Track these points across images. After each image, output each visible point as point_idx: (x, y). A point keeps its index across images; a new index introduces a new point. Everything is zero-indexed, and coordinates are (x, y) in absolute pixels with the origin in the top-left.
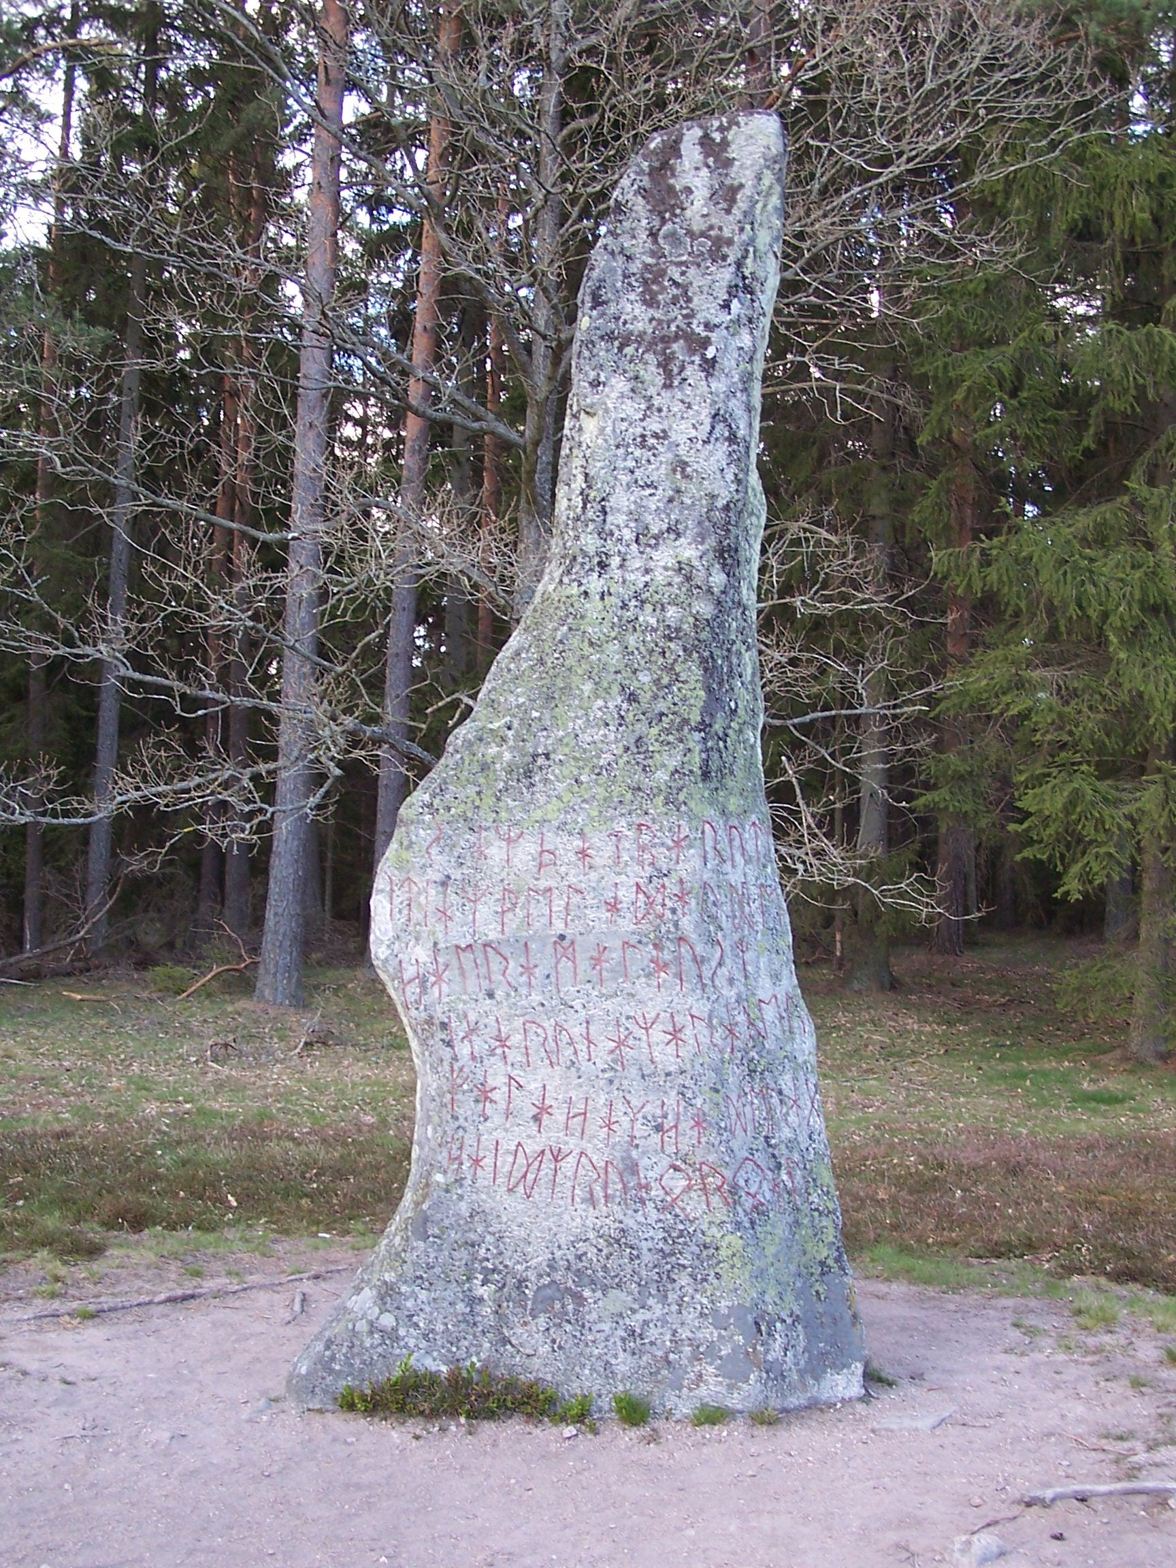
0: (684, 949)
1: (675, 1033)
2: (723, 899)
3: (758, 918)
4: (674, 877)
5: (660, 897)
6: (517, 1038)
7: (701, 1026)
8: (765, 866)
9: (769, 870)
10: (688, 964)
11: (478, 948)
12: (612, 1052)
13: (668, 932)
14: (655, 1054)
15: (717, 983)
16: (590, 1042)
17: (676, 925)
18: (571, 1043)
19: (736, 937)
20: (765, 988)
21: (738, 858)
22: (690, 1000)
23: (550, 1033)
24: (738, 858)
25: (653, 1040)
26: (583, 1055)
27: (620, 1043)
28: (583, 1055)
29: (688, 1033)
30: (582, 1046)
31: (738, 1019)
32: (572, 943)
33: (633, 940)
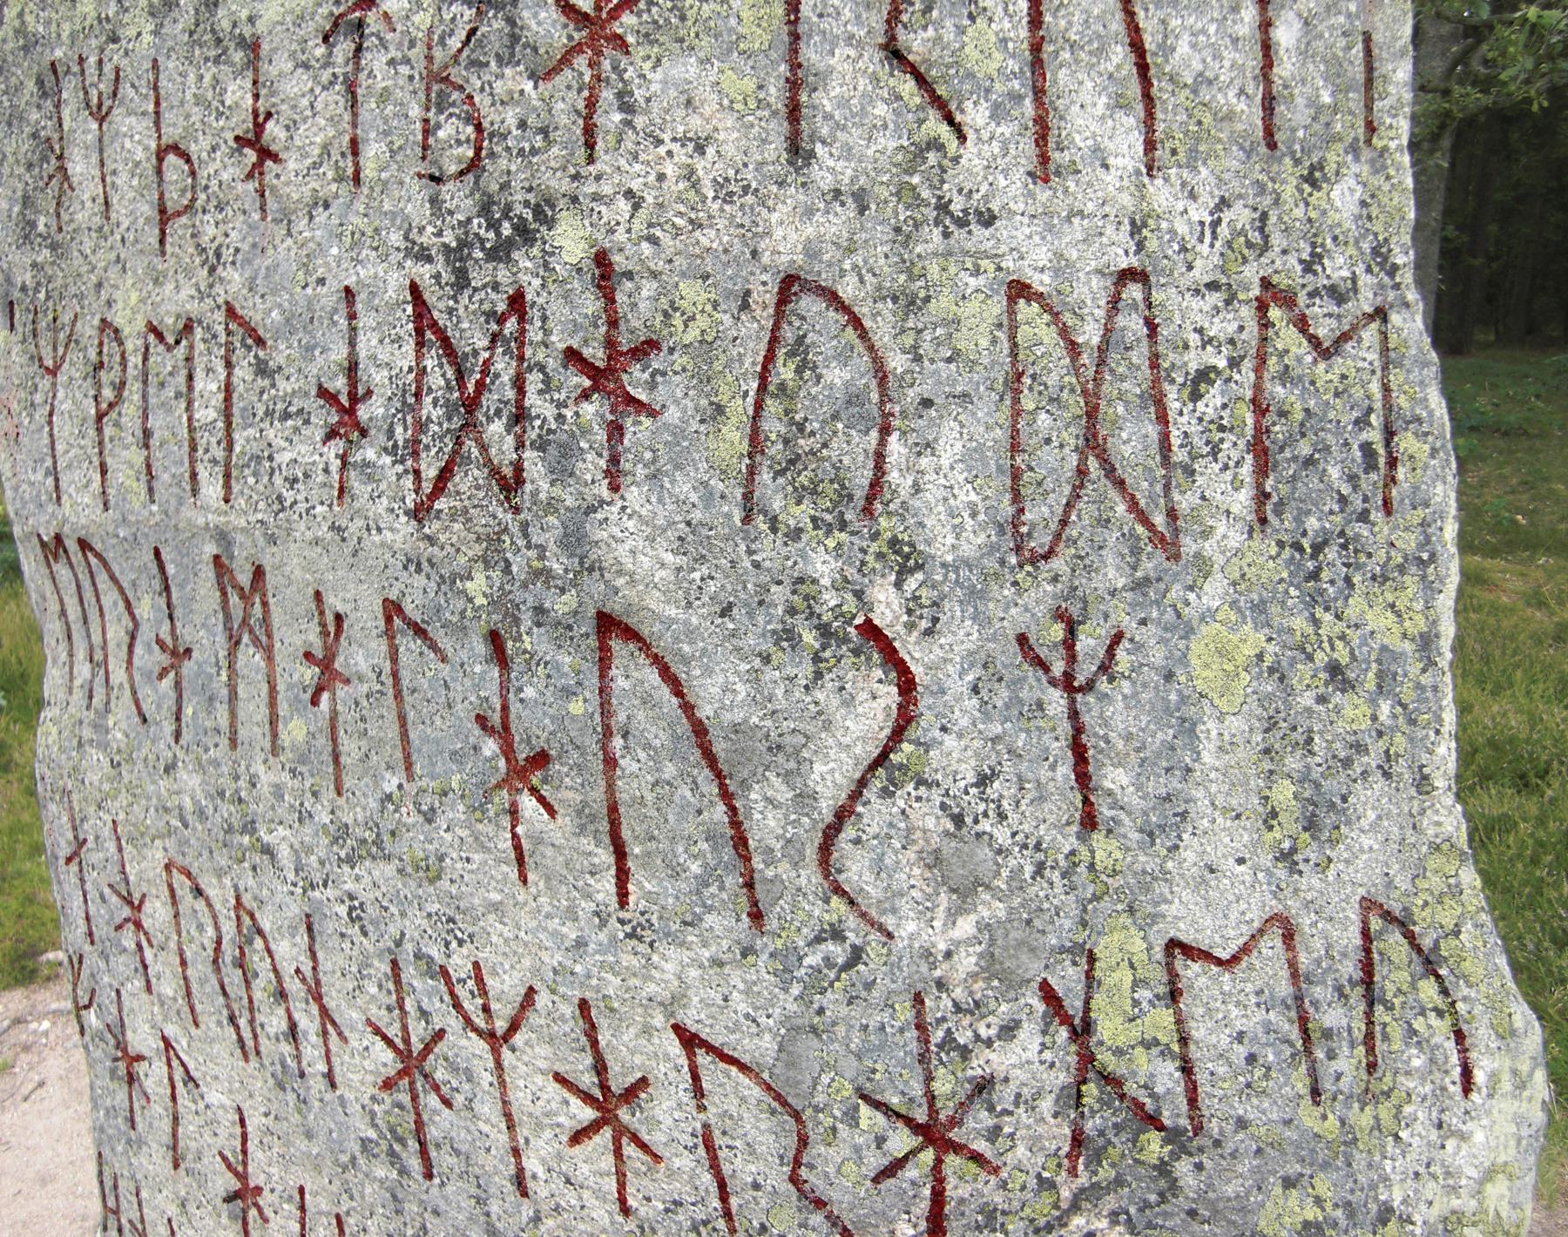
0: (632, 675)
1: (611, 1105)
2: (936, 377)
3: (1224, 490)
4: (570, 241)
5: (504, 367)
6: (157, 913)
7: (733, 1094)
8: (1313, 178)
9: (1343, 198)
10: (651, 767)
11: (72, 546)
12: (388, 1085)
13: (544, 574)
14: (532, 1164)
15: (856, 869)
16: (324, 1012)
17: (574, 540)
18: (282, 995)
19: (1029, 605)
20: (1216, 887)
21: (1093, 116)
22: (670, 962)
23: (228, 928)
24: (1093, 116)
25: (520, 1098)
26: (312, 1050)
27: (412, 1064)
28: (312, 1050)
29: (666, 1115)
30: (308, 1023)
31: (997, 1060)
32: (259, 573)
33: (417, 595)
